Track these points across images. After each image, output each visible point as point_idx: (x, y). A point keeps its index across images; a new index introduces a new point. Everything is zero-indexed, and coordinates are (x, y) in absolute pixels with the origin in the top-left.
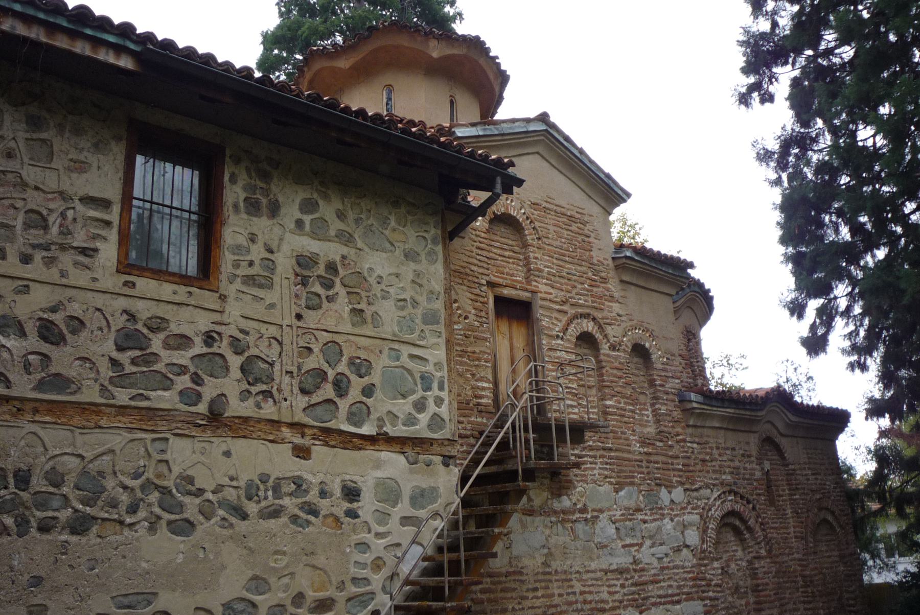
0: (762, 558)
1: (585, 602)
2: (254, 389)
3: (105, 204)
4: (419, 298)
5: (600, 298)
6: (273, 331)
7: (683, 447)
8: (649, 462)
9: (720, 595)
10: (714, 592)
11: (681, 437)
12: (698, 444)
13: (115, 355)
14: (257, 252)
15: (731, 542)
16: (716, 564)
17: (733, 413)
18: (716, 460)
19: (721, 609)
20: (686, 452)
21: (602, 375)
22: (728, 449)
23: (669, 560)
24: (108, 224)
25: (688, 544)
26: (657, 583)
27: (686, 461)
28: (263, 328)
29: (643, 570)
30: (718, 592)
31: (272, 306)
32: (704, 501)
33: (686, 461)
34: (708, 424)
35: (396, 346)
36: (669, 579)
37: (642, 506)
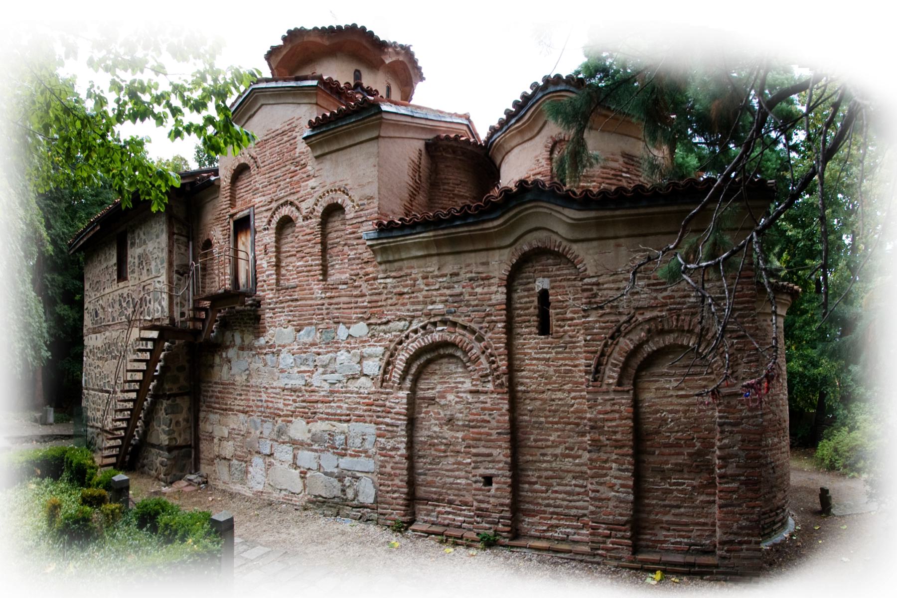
0: (486, 393)
5: (298, 182)
7: (372, 285)
8: (331, 304)
9: (400, 422)
10: (392, 419)
11: (371, 276)
12: (395, 278)
15: (456, 373)
17: (434, 236)
19: (400, 436)
20: (375, 289)
22: (446, 276)
23: (341, 385)
25: (365, 373)
26: (326, 403)
27: (375, 298)
29: (312, 391)
30: (400, 420)
32: (394, 333)
33: (375, 298)
34: (404, 255)
36: (339, 401)
37: (318, 341)
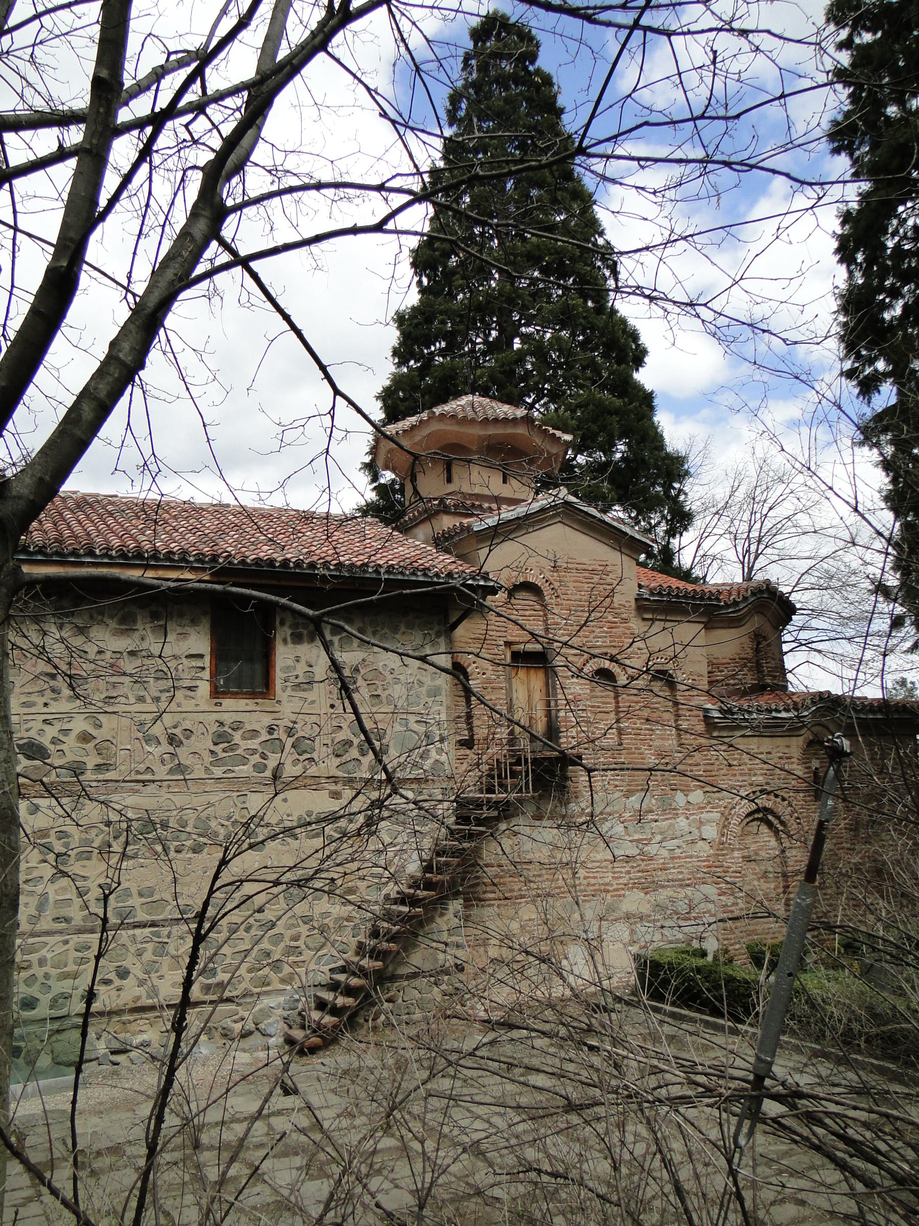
1: (589, 884)
2: (301, 758)
3: (201, 656)
4: (424, 679)
6: (314, 718)
13: (213, 748)
14: (301, 669)
16: (736, 854)
18: (746, 764)
21: (617, 702)
24: (203, 668)
27: (709, 767)
28: (307, 718)
31: (313, 702)
33: (709, 767)
35: (404, 716)
